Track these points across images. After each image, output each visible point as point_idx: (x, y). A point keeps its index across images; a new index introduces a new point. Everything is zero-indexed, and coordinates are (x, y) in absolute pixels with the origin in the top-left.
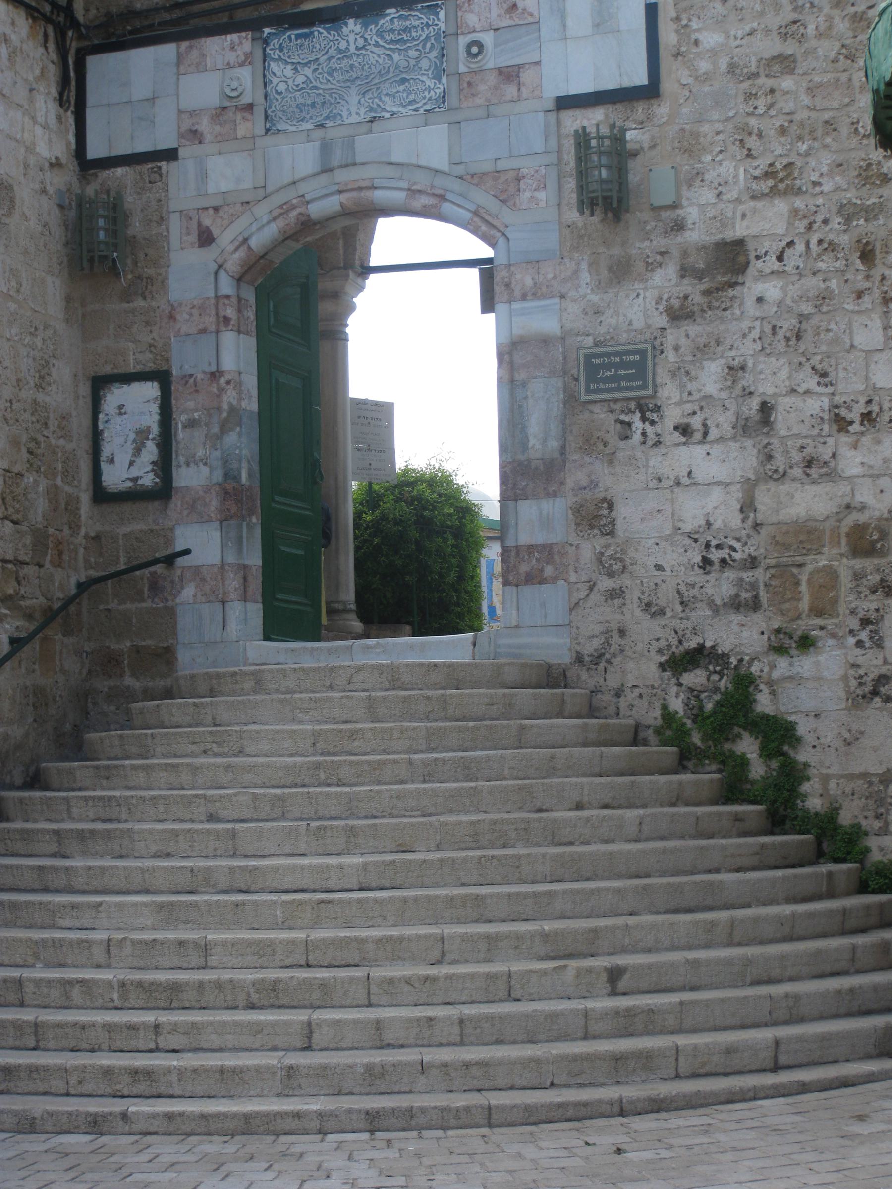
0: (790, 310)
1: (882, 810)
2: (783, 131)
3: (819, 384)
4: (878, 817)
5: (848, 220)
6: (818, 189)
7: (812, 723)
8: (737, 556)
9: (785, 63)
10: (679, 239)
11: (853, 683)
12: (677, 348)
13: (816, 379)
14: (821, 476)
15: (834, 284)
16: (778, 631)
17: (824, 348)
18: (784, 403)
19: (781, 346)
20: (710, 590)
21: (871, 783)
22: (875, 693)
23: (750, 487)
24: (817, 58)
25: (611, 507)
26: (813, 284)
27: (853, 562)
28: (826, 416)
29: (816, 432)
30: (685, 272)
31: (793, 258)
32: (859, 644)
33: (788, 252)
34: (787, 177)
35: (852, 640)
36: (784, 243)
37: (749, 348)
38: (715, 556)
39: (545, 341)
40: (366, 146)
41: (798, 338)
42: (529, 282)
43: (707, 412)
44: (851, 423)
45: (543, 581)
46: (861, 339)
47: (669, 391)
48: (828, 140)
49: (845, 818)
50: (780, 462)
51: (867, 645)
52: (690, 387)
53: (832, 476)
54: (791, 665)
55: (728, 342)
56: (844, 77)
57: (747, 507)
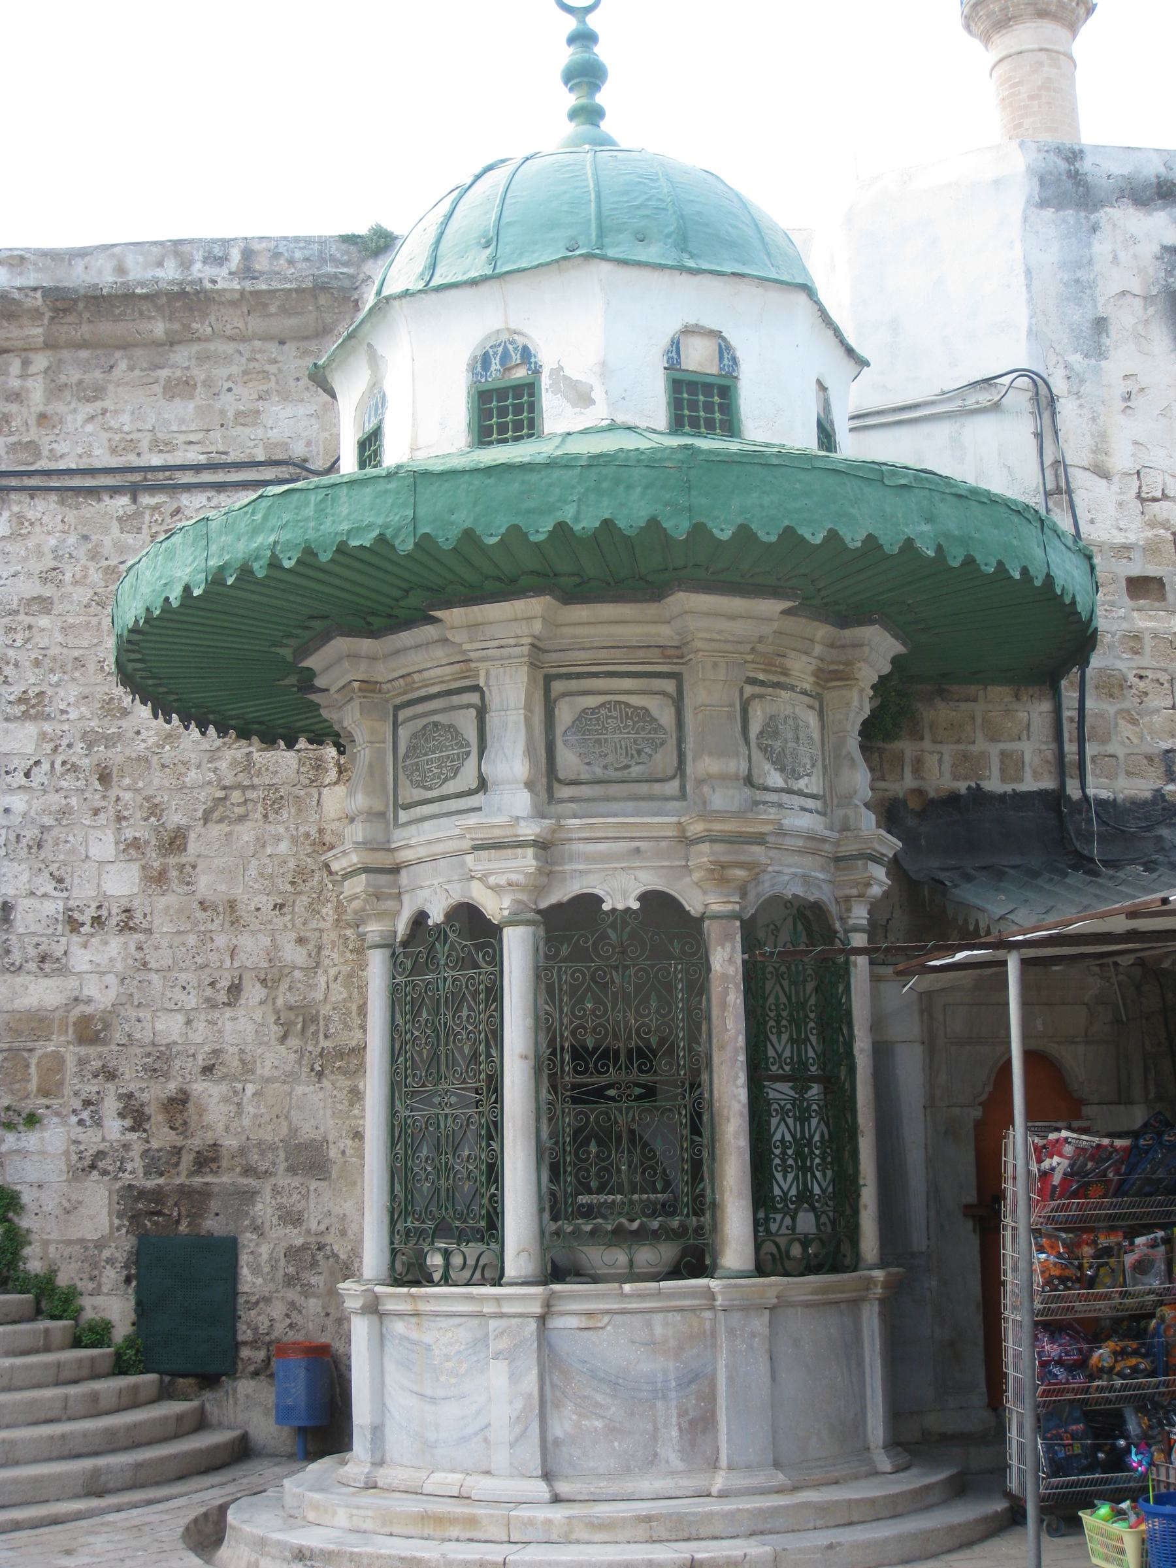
0: (33, 821)
1: (96, 1273)
2: (37, 663)
3: (55, 888)
4: (92, 1279)
5: (90, 746)
6: (65, 717)
7: (36, 1193)
9: (43, 604)
11: (74, 1157)
13: (54, 884)
14: (53, 970)
15: (74, 801)
16: (8, 1108)
17: (62, 857)
18: (23, 904)
19: (23, 853)
21: (86, 1248)
22: (93, 1167)
24: (71, 602)
26: (56, 800)
27: (78, 1049)
28: (61, 919)
29: (50, 931)
31: (40, 776)
32: (81, 1122)
33: (35, 770)
34: (38, 704)
35: (74, 1119)
36: (31, 762)
41: (40, 846)
44: (83, 925)
46: (95, 851)
48: (77, 674)
49: (62, 1280)
51: (88, 1124)
53: (63, 970)
54: (18, 1139)
56: (94, 621)
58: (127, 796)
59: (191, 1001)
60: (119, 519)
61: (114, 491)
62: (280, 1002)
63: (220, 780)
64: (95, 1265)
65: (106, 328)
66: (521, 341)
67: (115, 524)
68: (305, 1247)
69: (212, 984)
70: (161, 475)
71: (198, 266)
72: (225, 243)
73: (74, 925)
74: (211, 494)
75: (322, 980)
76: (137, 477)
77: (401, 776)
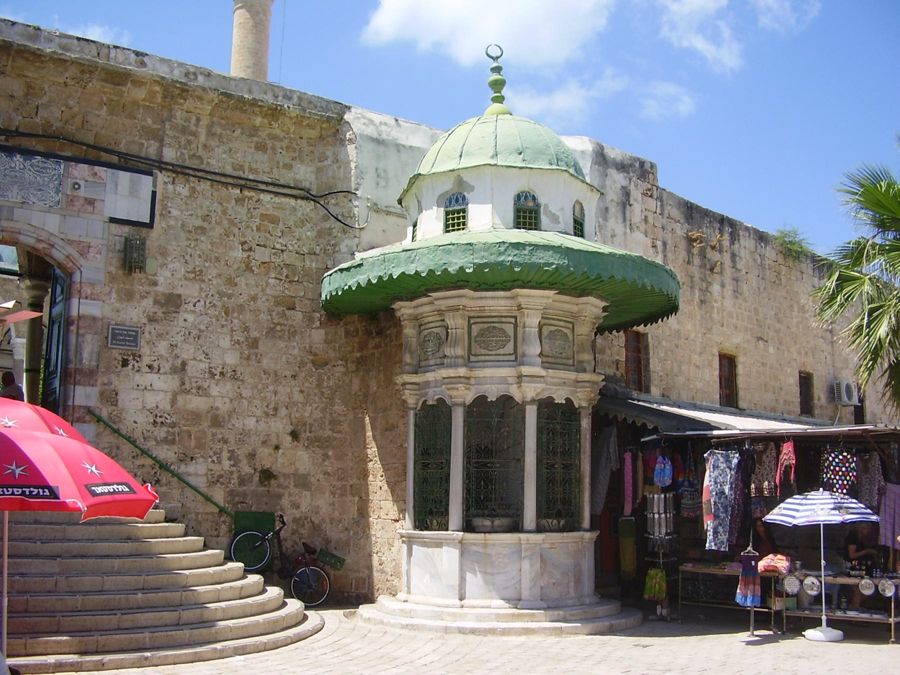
0: (196, 327)
4: (216, 530)
8: (168, 421)
9: (202, 230)
10: (155, 288)
12: (150, 333)
20: (155, 433)
23: (175, 396)
25: (117, 394)
30: (156, 302)
37: (179, 338)
38: (159, 420)
39: (94, 319)
40: (18, 212)
42: (89, 292)
43: (160, 361)
45: (84, 422)
47: (145, 350)
50: (187, 386)
52: (154, 349)
53: (207, 395)
55: (171, 334)
57: (173, 402)
58: (236, 321)
59: (259, 413)
60: (235, 199)
61: (234, 186)
62: (293, 416)
63: (272, 319)
64: (217, 524)
65: (237, 116)
66: (532, 193)
67: (234, 201)
68: (300, 518)
69: (267, 406)
70: (253, 184)
71: (280, 98)
72: (291, 91)
73: (213, 375)
74: (272, 196)
75: (309, 409)
76: (243, 182)
77: (473, 343)
